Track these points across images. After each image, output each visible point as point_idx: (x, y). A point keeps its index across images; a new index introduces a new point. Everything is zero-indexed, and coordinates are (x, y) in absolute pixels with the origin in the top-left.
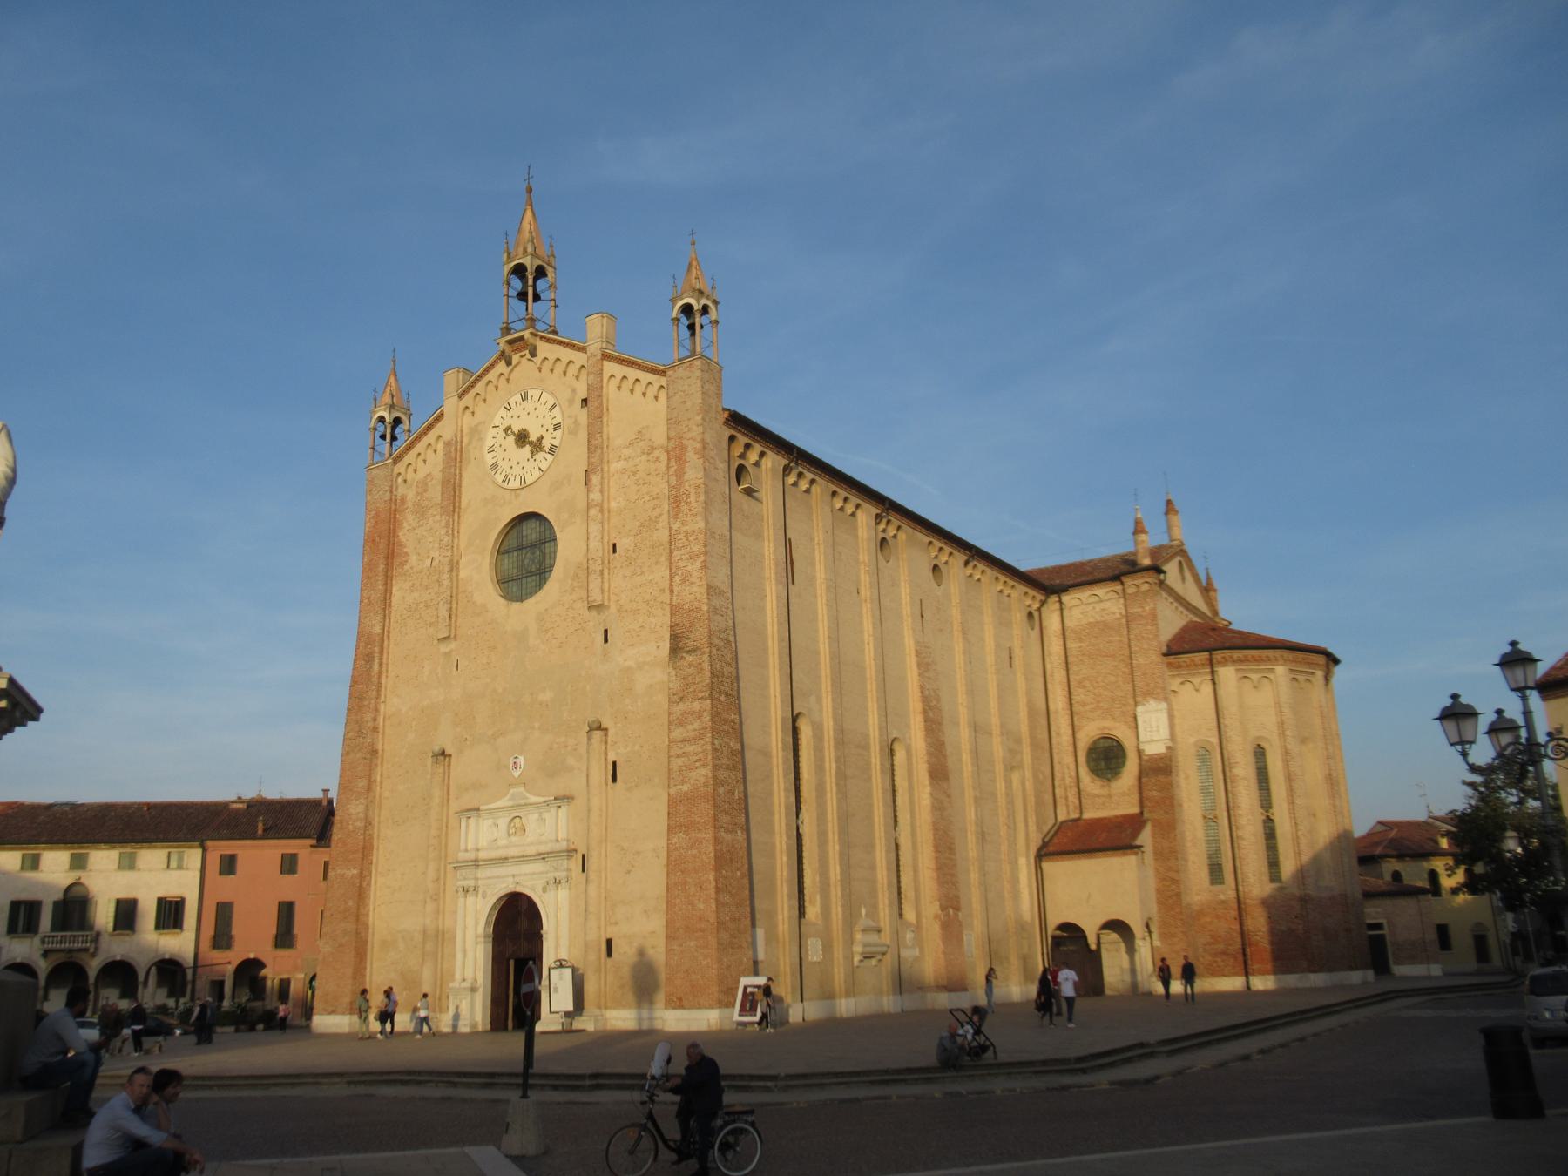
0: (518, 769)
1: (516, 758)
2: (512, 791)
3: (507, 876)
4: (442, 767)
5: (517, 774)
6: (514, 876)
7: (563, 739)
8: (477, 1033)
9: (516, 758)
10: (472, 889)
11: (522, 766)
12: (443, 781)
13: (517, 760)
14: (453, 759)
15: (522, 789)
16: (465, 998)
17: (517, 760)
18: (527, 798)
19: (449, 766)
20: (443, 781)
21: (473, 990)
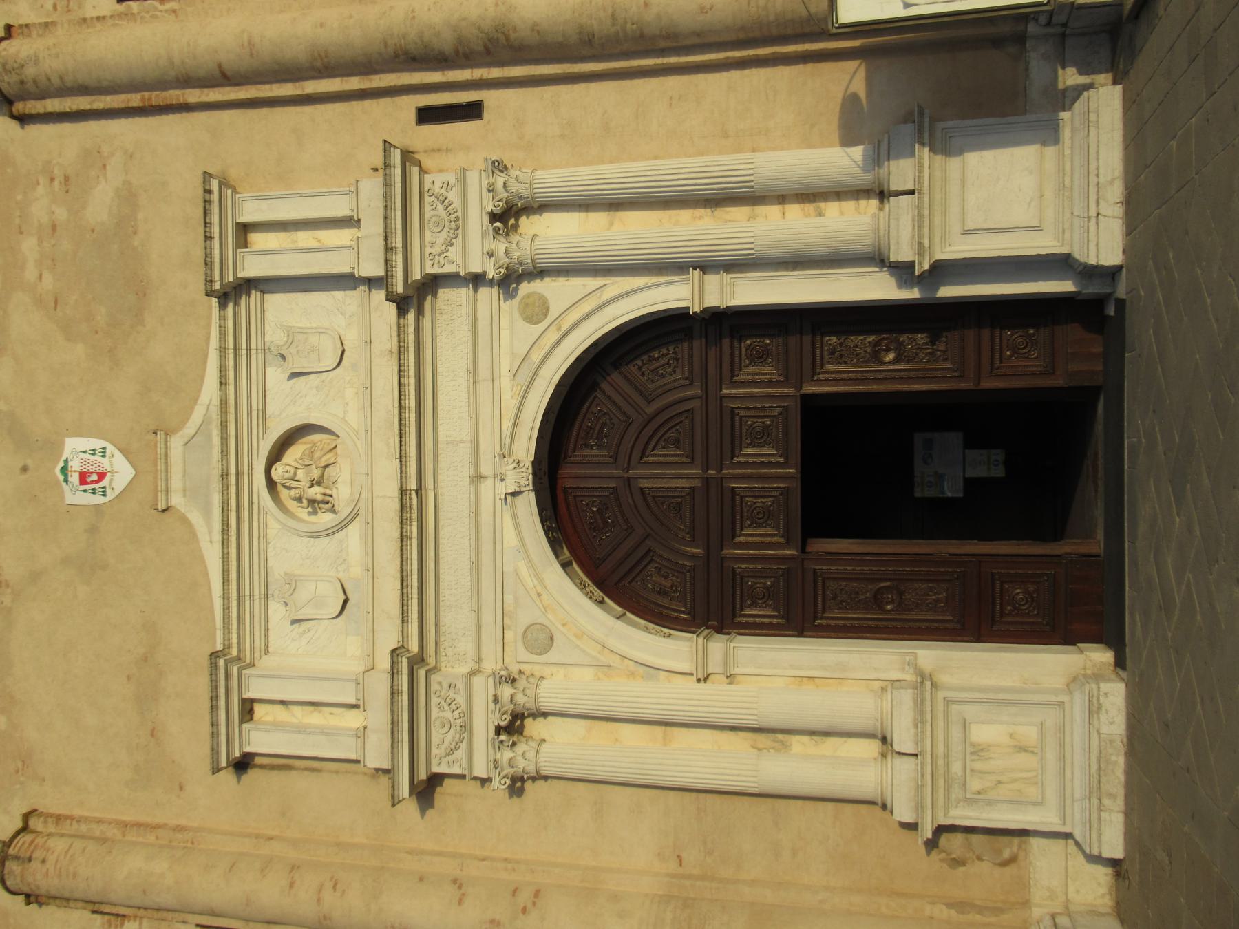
0: (105, 464)
1: (64, 470)
2: (177, 500)
3: (476, 514)
4: (52, 843)
5: (121, 472)
6: (478, 477)
7: (29, 246)
8: (1120, 663)
9: (64, 470)
10: (506, 691)
11: (98, 444)
12: (103, 840)
13: (75, 465)
14: (51, 802)
15: (176, 443)
16: (965, 726)
17: (75, 465)
18: (206, 421)
19: (59, 818)
20: (103, 840)
21: (924, 681)
